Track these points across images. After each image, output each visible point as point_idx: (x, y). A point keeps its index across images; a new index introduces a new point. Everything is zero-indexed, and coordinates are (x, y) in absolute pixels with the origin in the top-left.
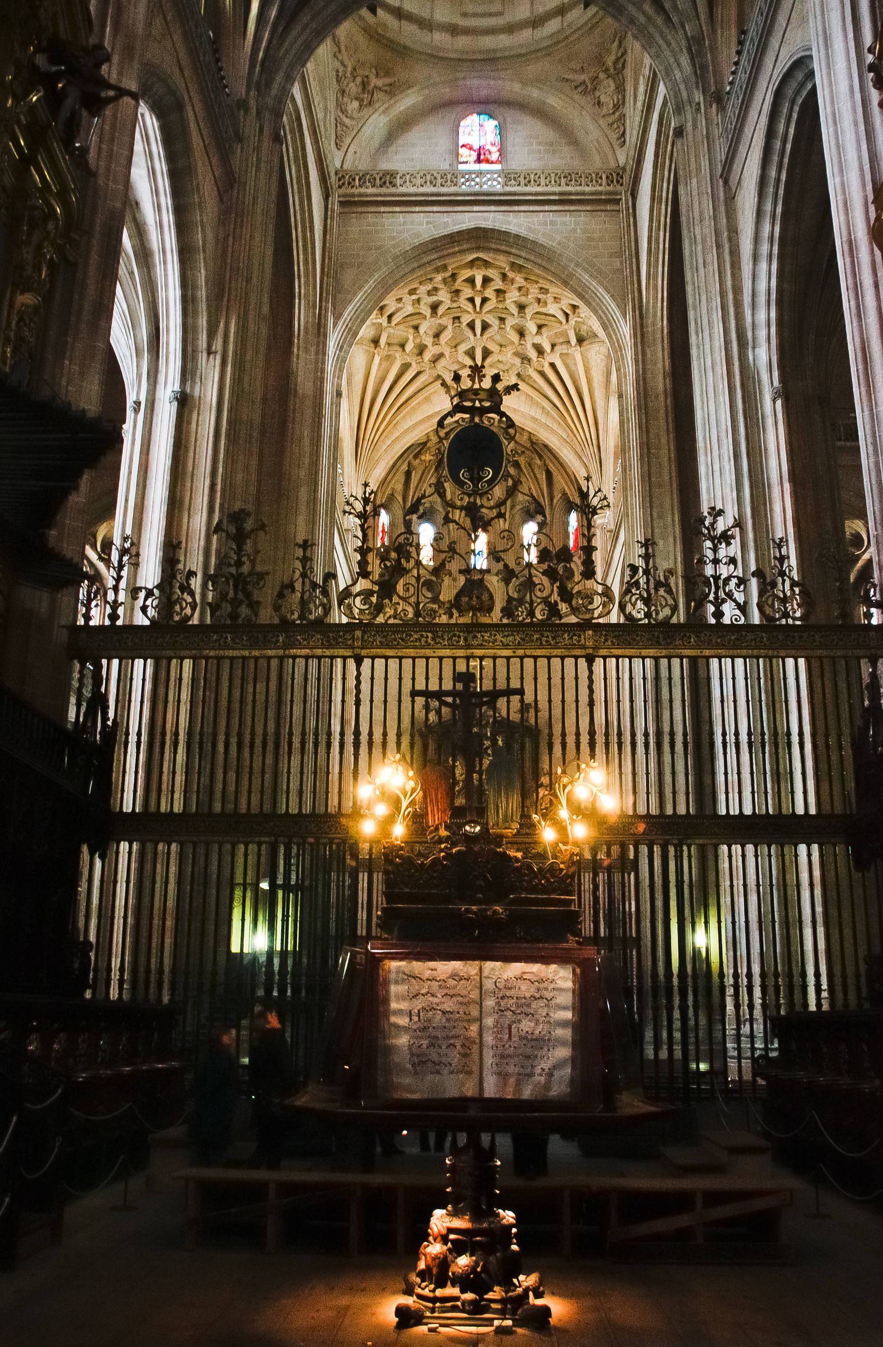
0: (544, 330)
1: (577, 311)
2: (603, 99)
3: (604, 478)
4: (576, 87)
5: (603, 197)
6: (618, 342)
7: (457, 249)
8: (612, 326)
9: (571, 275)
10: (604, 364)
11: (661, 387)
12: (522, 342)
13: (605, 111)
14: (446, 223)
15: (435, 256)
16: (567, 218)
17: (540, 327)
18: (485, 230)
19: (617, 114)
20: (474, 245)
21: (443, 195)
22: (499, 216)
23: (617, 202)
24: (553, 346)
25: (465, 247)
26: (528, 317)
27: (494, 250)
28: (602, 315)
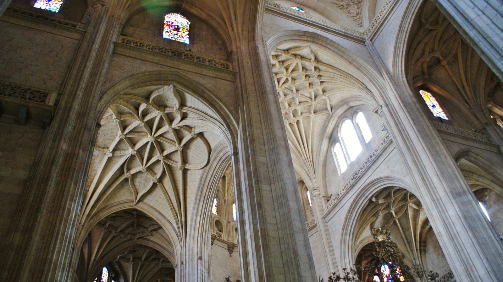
0: (302, 104)
1: (324, 93)
2: (351, 11)
3: (317, 175)
4: (339, 6)
5: (359, 39)
6: (379, 86)
7: (306, 39)
8: (375, 81)
9: (354, 60)
10: (322, 124)
11: (410, 101)
12: (290, 109)
13: (352, 15)
14: (303, 28)
15: (298, 38)
16: (348, 41)
17: (300, 103)
18: (318, 35)
19: (358, 17)
20: (312, 40)
21: (301, 18)
22: (323, 32)
23: (364, 42)
24: (301, 113)
25: (309, 39)
26: (299, 95)
27: (320, 44)
28: (369, 76)
